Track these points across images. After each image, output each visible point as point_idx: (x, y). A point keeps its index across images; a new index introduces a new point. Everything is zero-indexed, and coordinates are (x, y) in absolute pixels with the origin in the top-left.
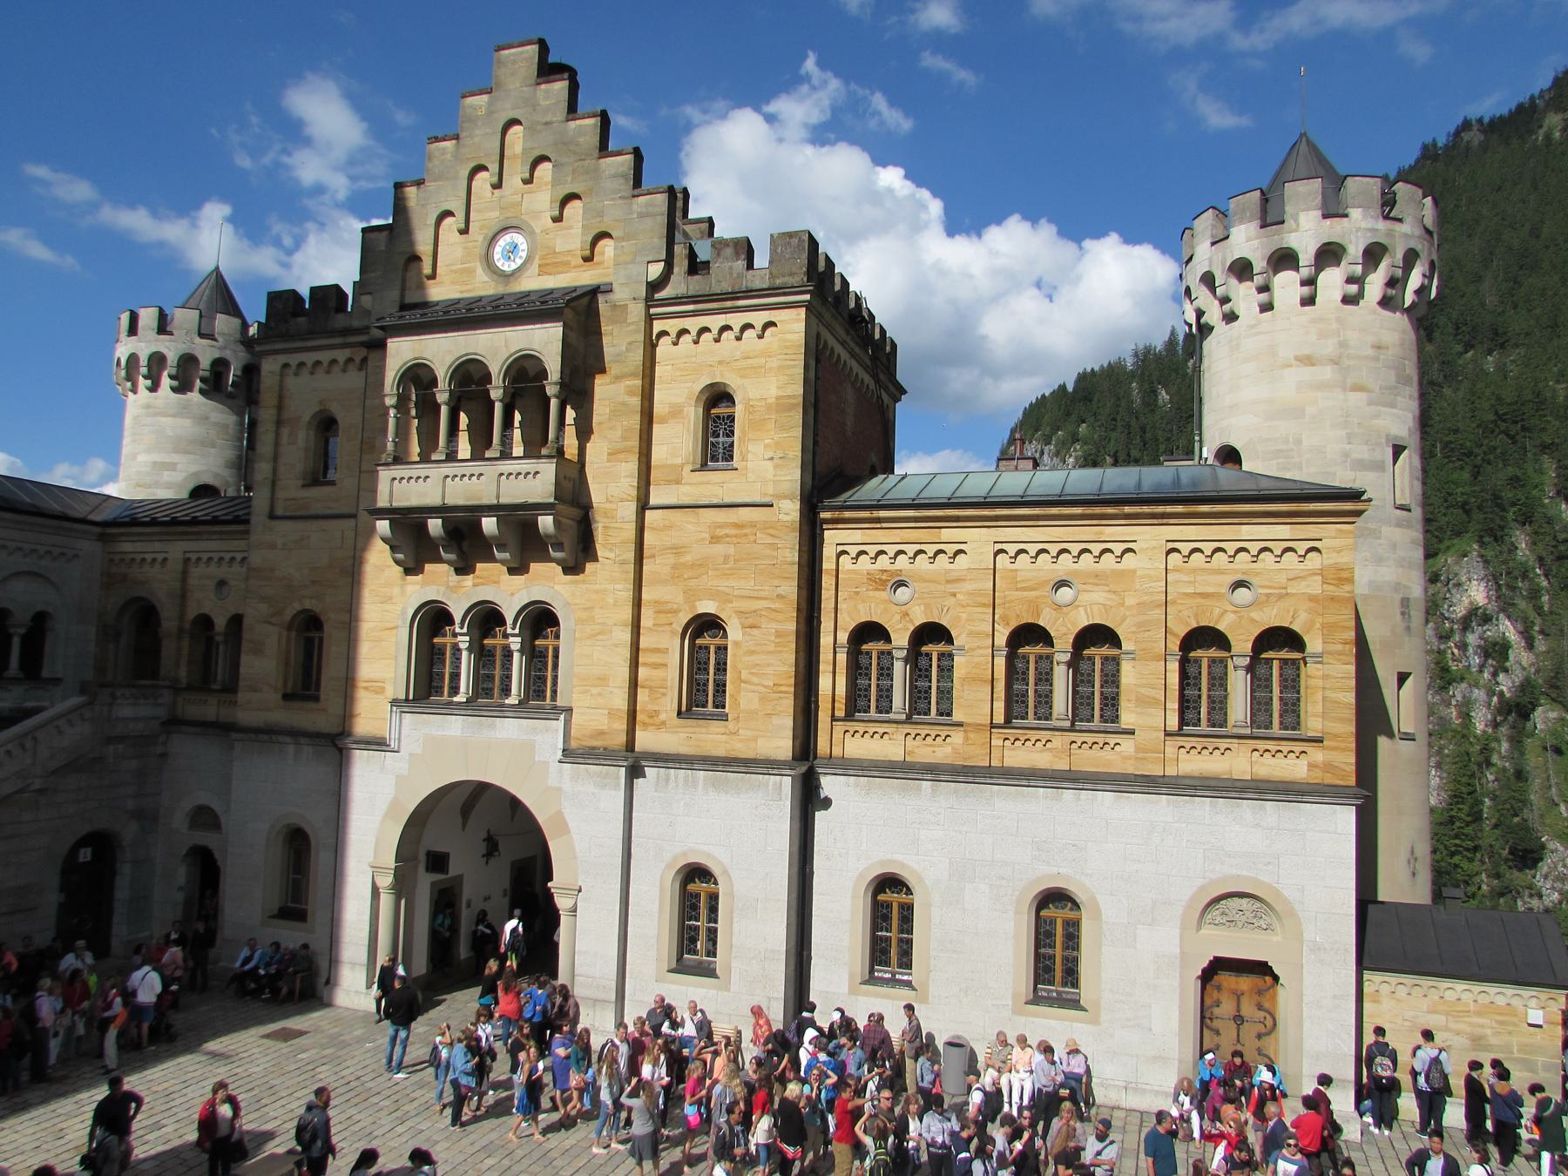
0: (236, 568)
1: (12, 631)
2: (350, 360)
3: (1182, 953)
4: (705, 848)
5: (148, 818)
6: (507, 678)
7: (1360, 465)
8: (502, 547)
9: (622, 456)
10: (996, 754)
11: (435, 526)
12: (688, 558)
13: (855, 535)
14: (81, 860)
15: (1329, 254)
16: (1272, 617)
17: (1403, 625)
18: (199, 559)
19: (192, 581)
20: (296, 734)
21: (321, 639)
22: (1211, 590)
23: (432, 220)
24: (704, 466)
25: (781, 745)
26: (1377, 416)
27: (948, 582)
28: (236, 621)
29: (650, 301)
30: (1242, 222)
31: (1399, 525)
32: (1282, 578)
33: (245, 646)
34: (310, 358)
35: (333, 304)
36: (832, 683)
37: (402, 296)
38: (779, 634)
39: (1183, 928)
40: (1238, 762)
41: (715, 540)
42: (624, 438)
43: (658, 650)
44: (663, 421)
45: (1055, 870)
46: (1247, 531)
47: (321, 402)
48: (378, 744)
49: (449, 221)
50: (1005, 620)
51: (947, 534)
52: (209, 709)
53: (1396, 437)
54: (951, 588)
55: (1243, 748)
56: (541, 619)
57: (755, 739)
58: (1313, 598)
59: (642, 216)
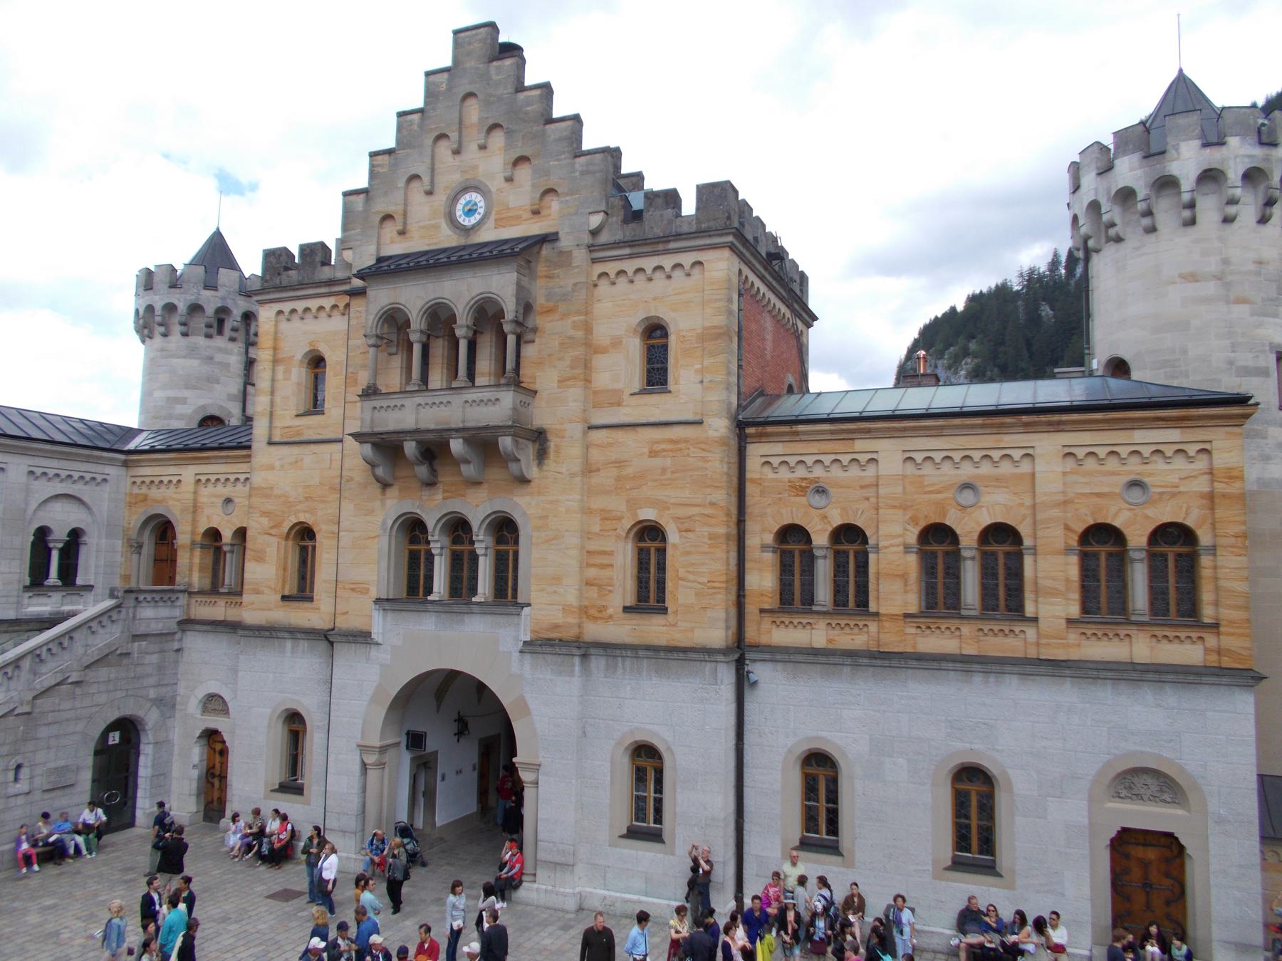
1: (51, 545)
2: (335, 307)
3: (1091, 824)
4: (651, 727)
5: (167, 705)
6: (474, 578)
7: (1247, 372)
8: (467, 462)
11: (410, 448)
12: (629, 471)
13: (779, 448)
14: (111, 743)
15: (1210, 177)
16: (1166, 513)
18: (208, 480)
19: (202, 500)
20: (295, 633)
21: (314, 548)
23: (401, 184)
24: (642, 392)
25: (717, 634)
26: (1260, 325)
27: (862, 487)
28: (241, 533)
29: (591, 248)
32: (1174, 479)
33: (248, 554)
34: (300, 305)
35: (318, 258)
36: (763, 579)
37: (378, 250)
39: (1091, 800)
41: (653, 454)
45: (968, 746)
46: (1139, 436)
47: (310, 344)
48: (362, 637)
49: (415, 184)
50: (914, 520)
51: (859, 445)
52: (218, 610)
55: (1141, 635)
56: (505, 528)
57: (692, 630)
59: (582, 173)
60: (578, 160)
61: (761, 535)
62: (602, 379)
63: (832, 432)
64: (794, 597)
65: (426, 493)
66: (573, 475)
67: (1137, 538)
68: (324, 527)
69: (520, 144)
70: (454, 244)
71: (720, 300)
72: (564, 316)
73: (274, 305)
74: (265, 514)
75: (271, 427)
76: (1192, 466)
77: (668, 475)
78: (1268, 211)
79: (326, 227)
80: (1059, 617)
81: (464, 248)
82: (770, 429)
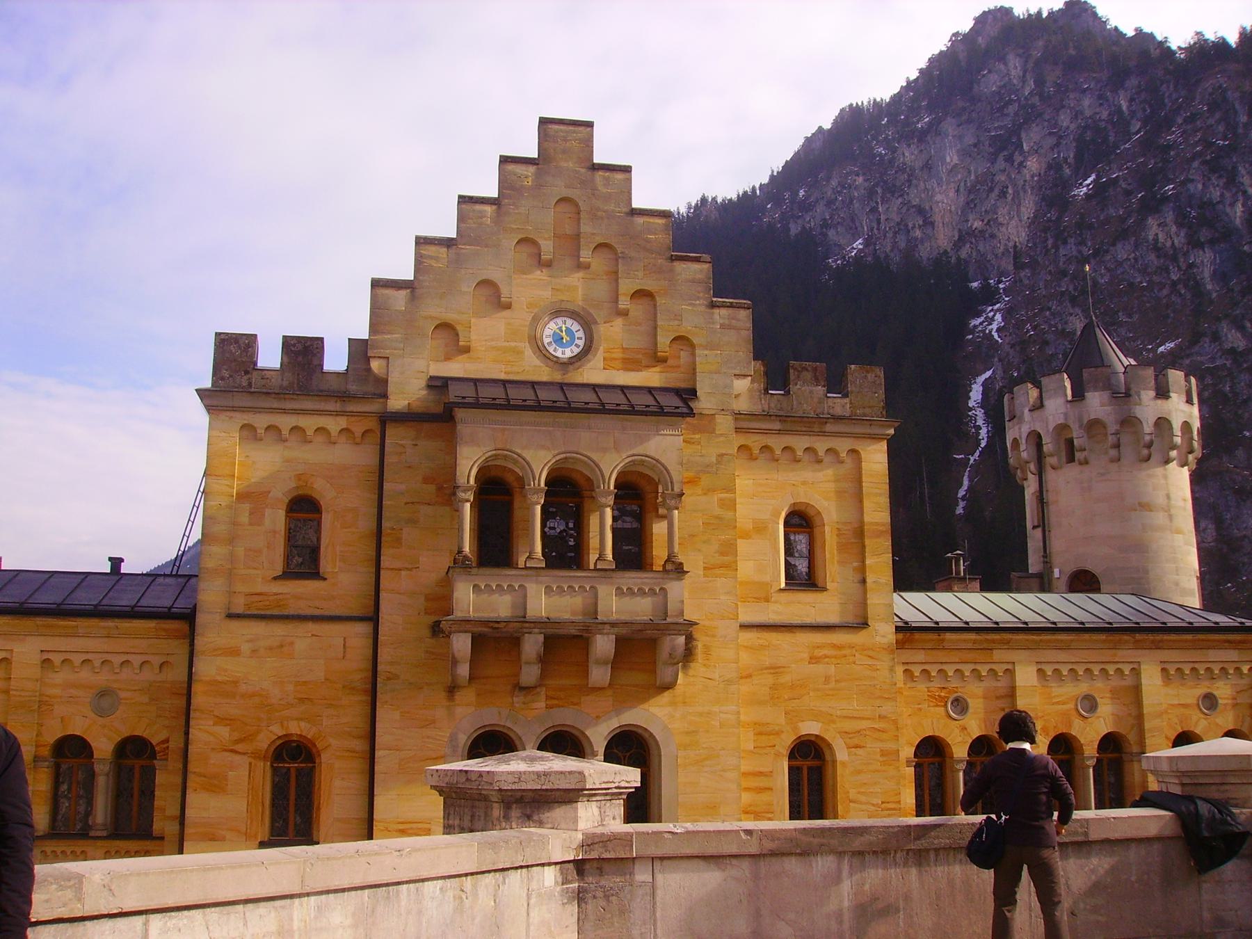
0: (126, 674)
9: (718, 571)
12: (786, 679)
13: (920, 656)
30: (1096, 389)
38: (884, 753)
41: (814, 660)
43: (761, 774)
44: (746, 535)
46: (1213, 655)
47: (299, 477)
51: (998, 655)
60: (716, 311)
62: (746, 569)
63: (975, 642)
65: (519, 699)
66: (729, 682)
68: (334, 742)
69: (640, 274)
70: (545, 379)
71: (880, 495)
72: (708, 491)
73: (237, 415)
74: (221, 720)
75: (232, 593)
77: (832, 685)
79: (341, 324)
81: (562, 386)
82: (917, 636)
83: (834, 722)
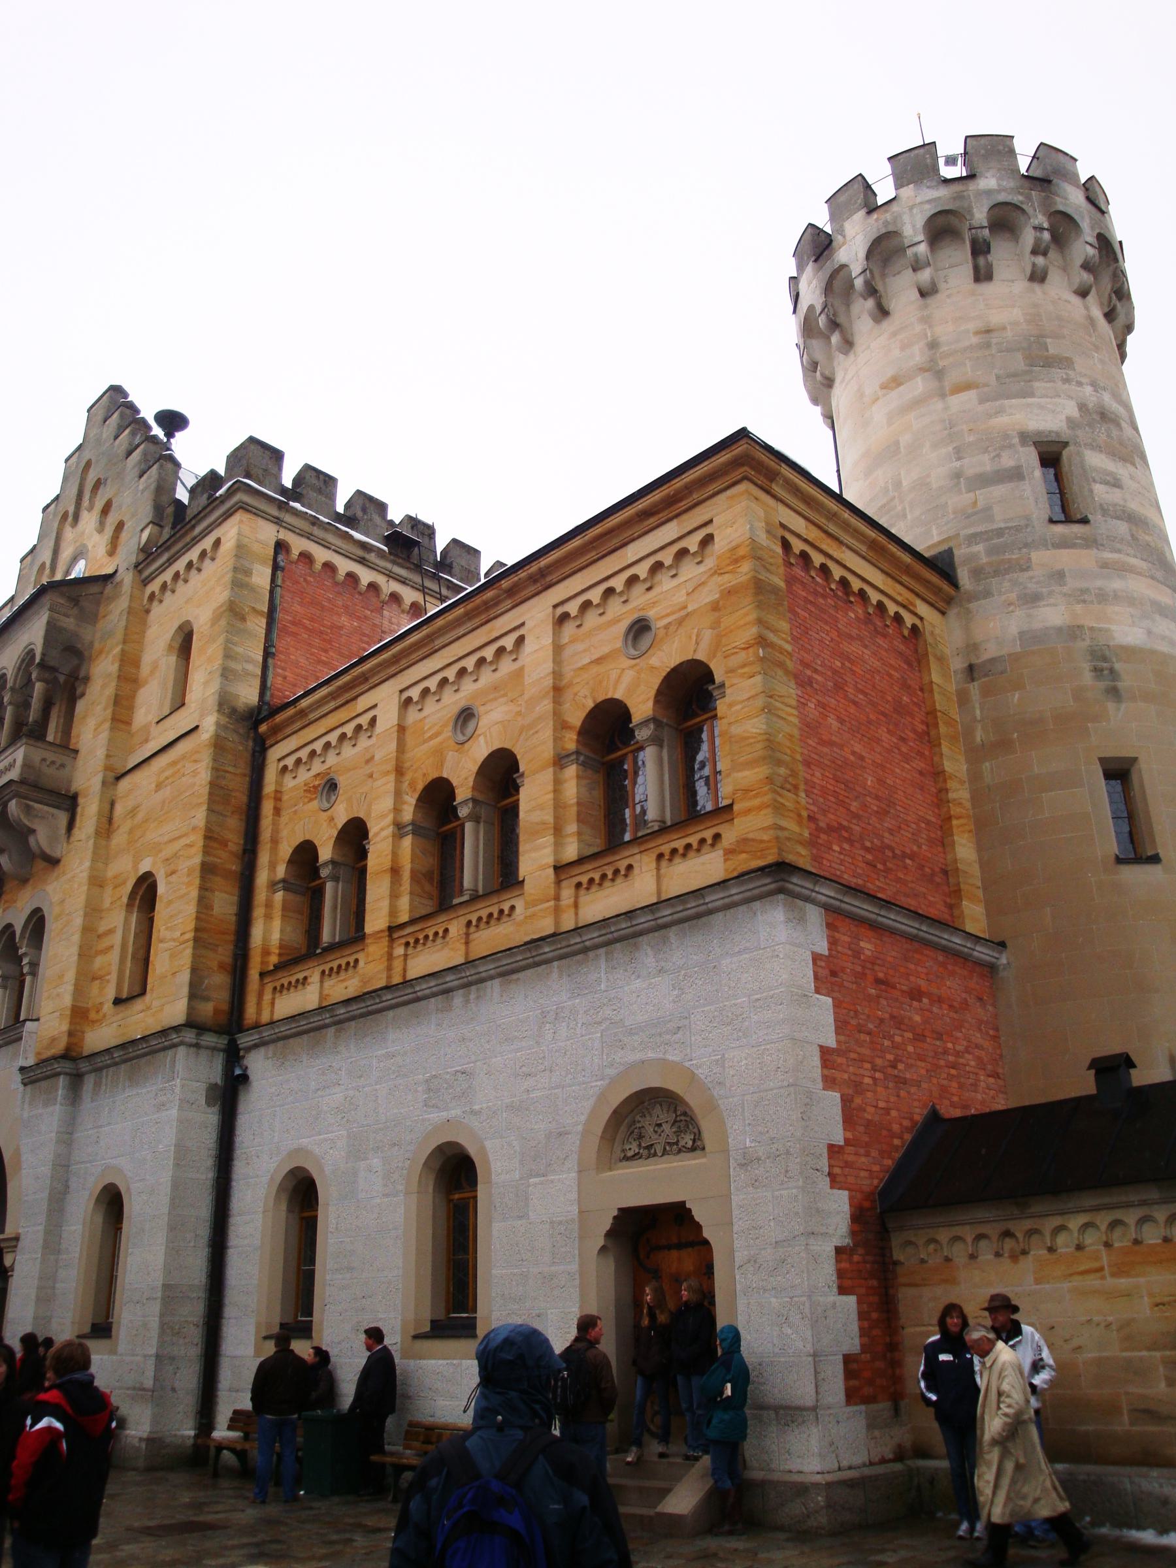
3: (581, 1212)
7: (983, 480)
10: (398, 965)
16: (668, 655)
17: (1102, 685)
22: (606, 650)
26: (1000, 412)
31: (1064, 544)
32: (680, 597)
36: (270, 931)
40: (641, 884)
41: (159, 787)
42: (105, 709)
45: (444, 1115)
46: (633, 552)
53: (1039, 433)
54: (368, 769)
58: (715, 607)
61: (272, 866)
63: (332, 696)
64: (307, 950)
67: (642, 707)
76: (702, 568)
78: (981, 261)
80: (543, 868)
83: (160, 851)
